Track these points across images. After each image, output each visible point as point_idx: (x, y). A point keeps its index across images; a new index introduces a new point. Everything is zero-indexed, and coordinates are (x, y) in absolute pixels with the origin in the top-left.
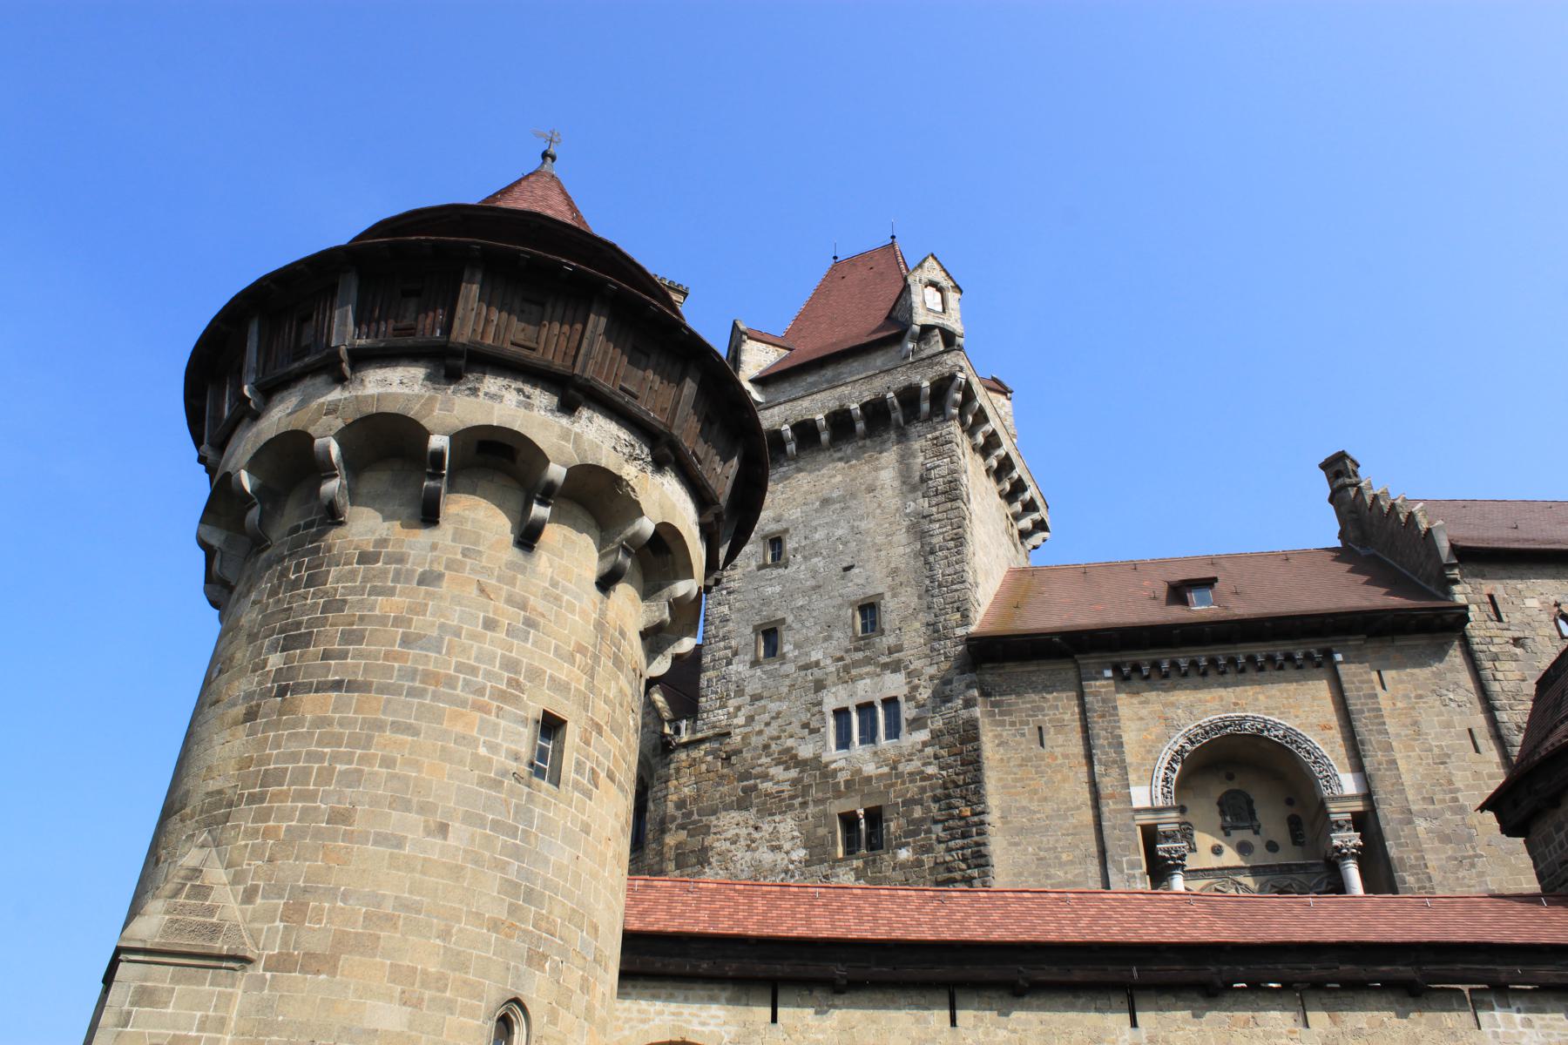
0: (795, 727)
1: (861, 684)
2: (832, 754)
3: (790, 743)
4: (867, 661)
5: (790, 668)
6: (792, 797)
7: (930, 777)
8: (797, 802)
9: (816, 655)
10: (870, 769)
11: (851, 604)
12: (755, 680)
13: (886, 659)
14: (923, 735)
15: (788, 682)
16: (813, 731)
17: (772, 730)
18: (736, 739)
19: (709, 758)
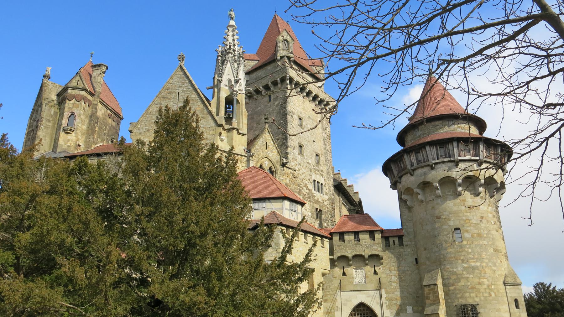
0: (307, 179)
1: (318, 176)
2: (313, 191)
3: (307, 182)
4: (318, 171)
5: (305, 161)
6: (308, 198)
7: (328, 208)
8: (309, 199)
9: (310, 162)
10: (320, 200)
11: (315, 152)
12: (299, 158)
13: (321, 173)
14: (326, 197)
15: (305, 164)
16: (311, 183)
17: (303, 176)
18: (296, 173)
19: (291, 175)
